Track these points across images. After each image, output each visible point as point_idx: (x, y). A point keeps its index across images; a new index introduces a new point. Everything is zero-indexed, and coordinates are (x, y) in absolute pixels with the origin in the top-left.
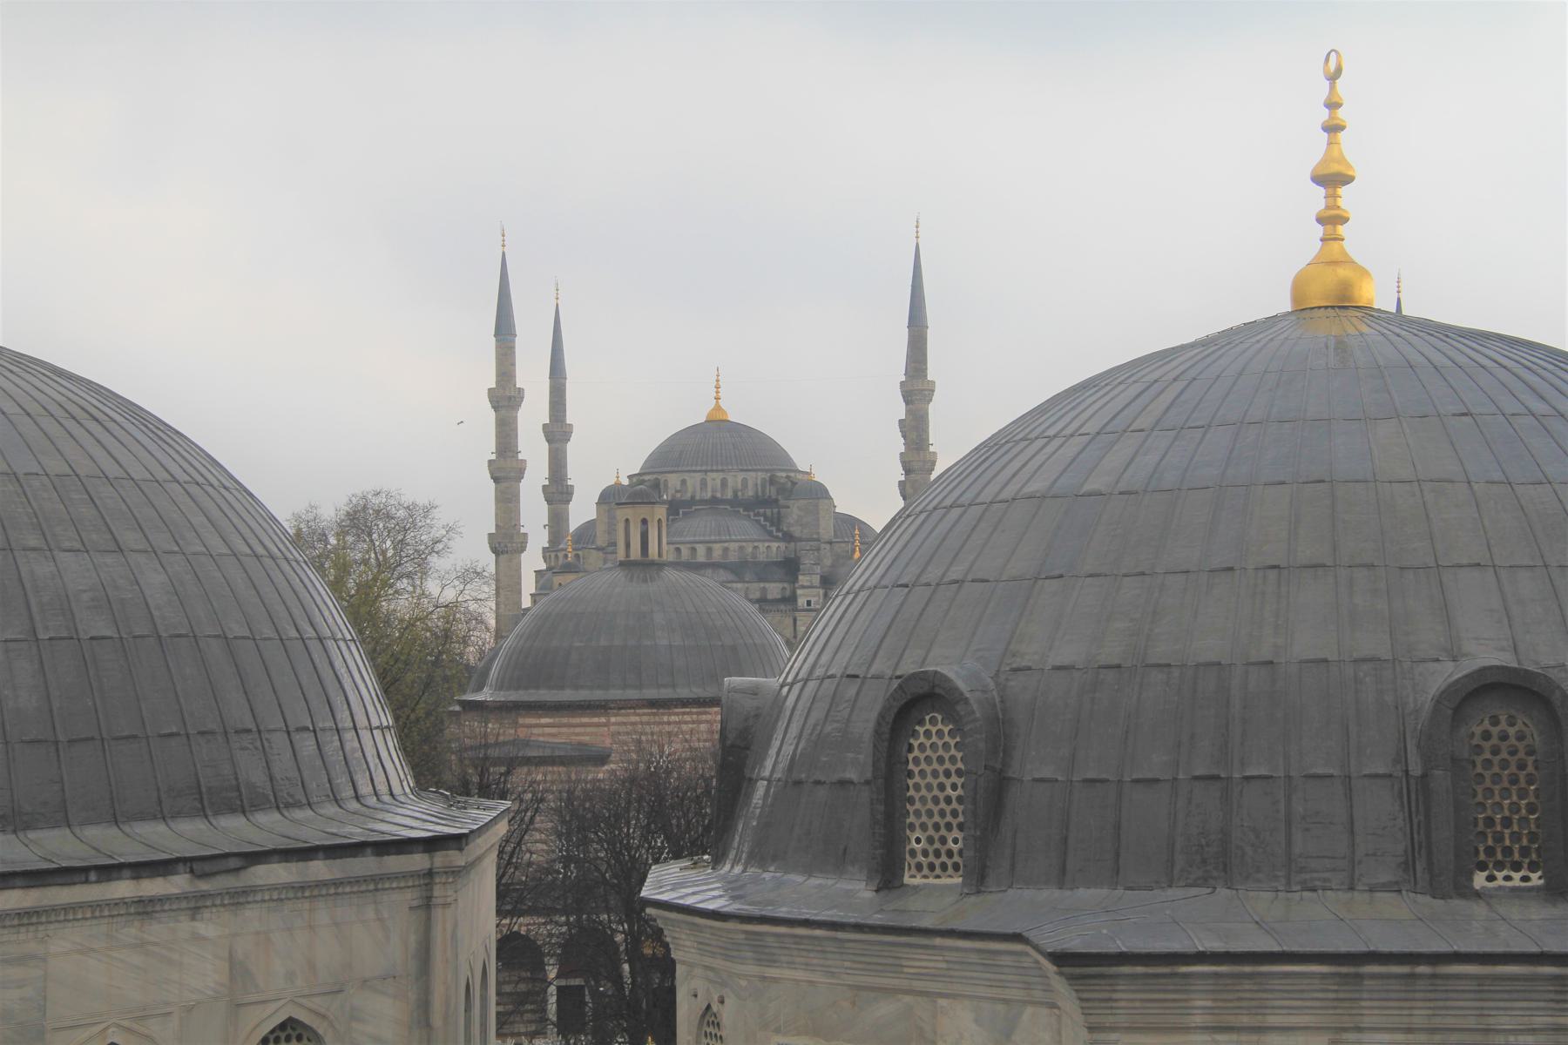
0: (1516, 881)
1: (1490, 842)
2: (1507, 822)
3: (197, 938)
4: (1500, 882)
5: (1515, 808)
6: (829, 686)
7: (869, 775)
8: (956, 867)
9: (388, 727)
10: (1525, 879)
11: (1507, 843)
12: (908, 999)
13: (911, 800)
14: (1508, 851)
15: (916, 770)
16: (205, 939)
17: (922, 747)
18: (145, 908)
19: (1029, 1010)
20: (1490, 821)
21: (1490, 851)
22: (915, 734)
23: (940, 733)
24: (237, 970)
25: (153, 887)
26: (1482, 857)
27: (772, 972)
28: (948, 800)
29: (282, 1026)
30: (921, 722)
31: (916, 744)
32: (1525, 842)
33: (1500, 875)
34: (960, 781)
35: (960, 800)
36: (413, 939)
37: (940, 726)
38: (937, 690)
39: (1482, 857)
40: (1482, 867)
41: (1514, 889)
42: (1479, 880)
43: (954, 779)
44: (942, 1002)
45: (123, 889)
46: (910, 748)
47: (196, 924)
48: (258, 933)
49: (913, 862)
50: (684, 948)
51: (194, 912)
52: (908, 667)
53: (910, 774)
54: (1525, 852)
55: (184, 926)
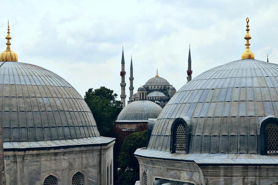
0: (274, 152)
1: (270, 146)
2: (273, 143)
3: (64, 159)
4: (272, 152)
5: (274, 141)
6: (164, 120)
7: (170, 135)
8: (184, 150)
9: (95, 126)
10: (276, 152)
11: (273, 146)
12: (176, 171)
13: (177, 139)
14: (273, 148)
15: (178, 134)
16: (65, 159)
17: (179, 130)
18: (56, 154)
19: (195, 173)
20: (270, 143)
21: (270, 148)
22: (178, 128)
23: (182, 128)
24: (71, 164)
25: (57, 151)
26: (269, 148)
27: (154, 166)
28: (183, 139)
29: (77, 173)
32: (276, 146)
33: (271, 151)
34: (185, 136)
35: (185, 139)
36: (98, 160)
38: (181, 121)
39: (269, 148)
41: (274, 154)
42: (268, 152)
43: (184, 135)
44: (181, 171)
45: (52, 151)
46: (177, 130)
47: (64, 157)
48: (73, 158)
49: (177, 149)
50: (141, 163)
51: (64, 155)
52: (177, 117)
53: (177, 135)
54: (276, 148)
55: (62, 157)
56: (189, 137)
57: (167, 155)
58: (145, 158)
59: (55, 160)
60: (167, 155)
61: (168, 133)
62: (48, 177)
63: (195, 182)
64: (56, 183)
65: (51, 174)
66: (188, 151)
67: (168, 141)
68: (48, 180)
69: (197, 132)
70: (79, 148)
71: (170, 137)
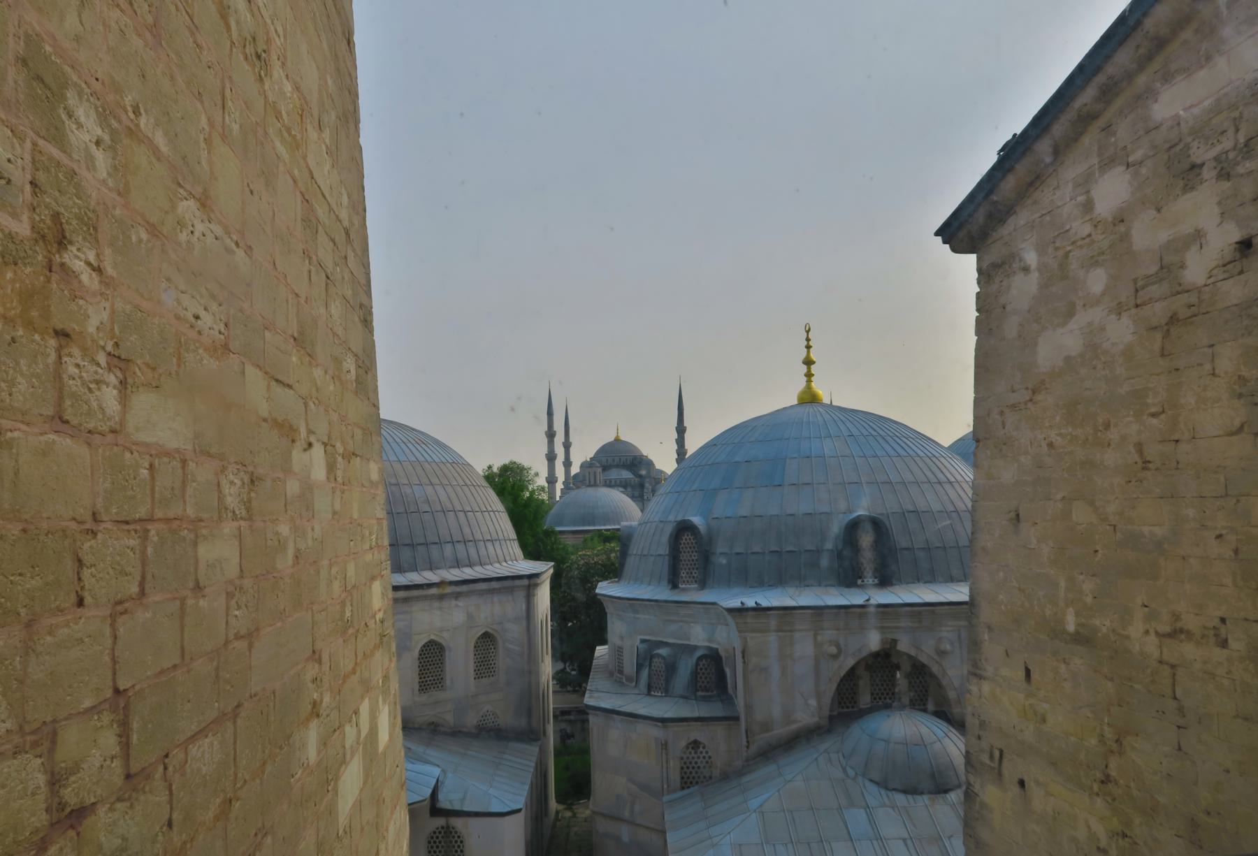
7: (667, 553)
8: (696, 581)
13: (681, 561)
17: (684, 544)
18: (441, 597)
19: (720, 627)
22: (682, 540)
24: (470, 617)
27: (637, 616)
28: (693, 560)
30: (684, 535)
31: (682, 542)
35: (696, 560)
37: (690, 537)
40: (860, 578)
44: (692, 625)
45: (434, 591)
46: (681, 544)
52: (680, 518)
55: (454, 602)
56: (706, 558)
57: (664, 594)
58: (620, 601)
59: (440, 608)
60: (664, 594)
61: (664, 549)
62: (426, 643)
63: (719, 644)
64: (441, 656)
65: (433, 637)
66: (703, 584)
67: (664, 566)
68: (426, 650)
69: (721, 547)
70: (486, 583)
71: (667, 558)
